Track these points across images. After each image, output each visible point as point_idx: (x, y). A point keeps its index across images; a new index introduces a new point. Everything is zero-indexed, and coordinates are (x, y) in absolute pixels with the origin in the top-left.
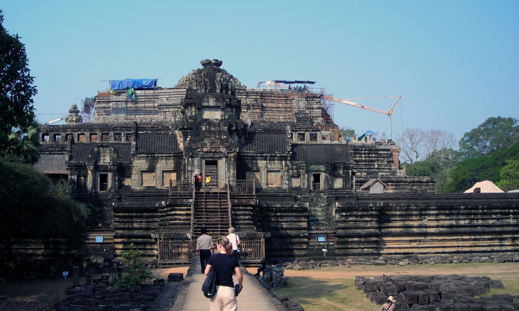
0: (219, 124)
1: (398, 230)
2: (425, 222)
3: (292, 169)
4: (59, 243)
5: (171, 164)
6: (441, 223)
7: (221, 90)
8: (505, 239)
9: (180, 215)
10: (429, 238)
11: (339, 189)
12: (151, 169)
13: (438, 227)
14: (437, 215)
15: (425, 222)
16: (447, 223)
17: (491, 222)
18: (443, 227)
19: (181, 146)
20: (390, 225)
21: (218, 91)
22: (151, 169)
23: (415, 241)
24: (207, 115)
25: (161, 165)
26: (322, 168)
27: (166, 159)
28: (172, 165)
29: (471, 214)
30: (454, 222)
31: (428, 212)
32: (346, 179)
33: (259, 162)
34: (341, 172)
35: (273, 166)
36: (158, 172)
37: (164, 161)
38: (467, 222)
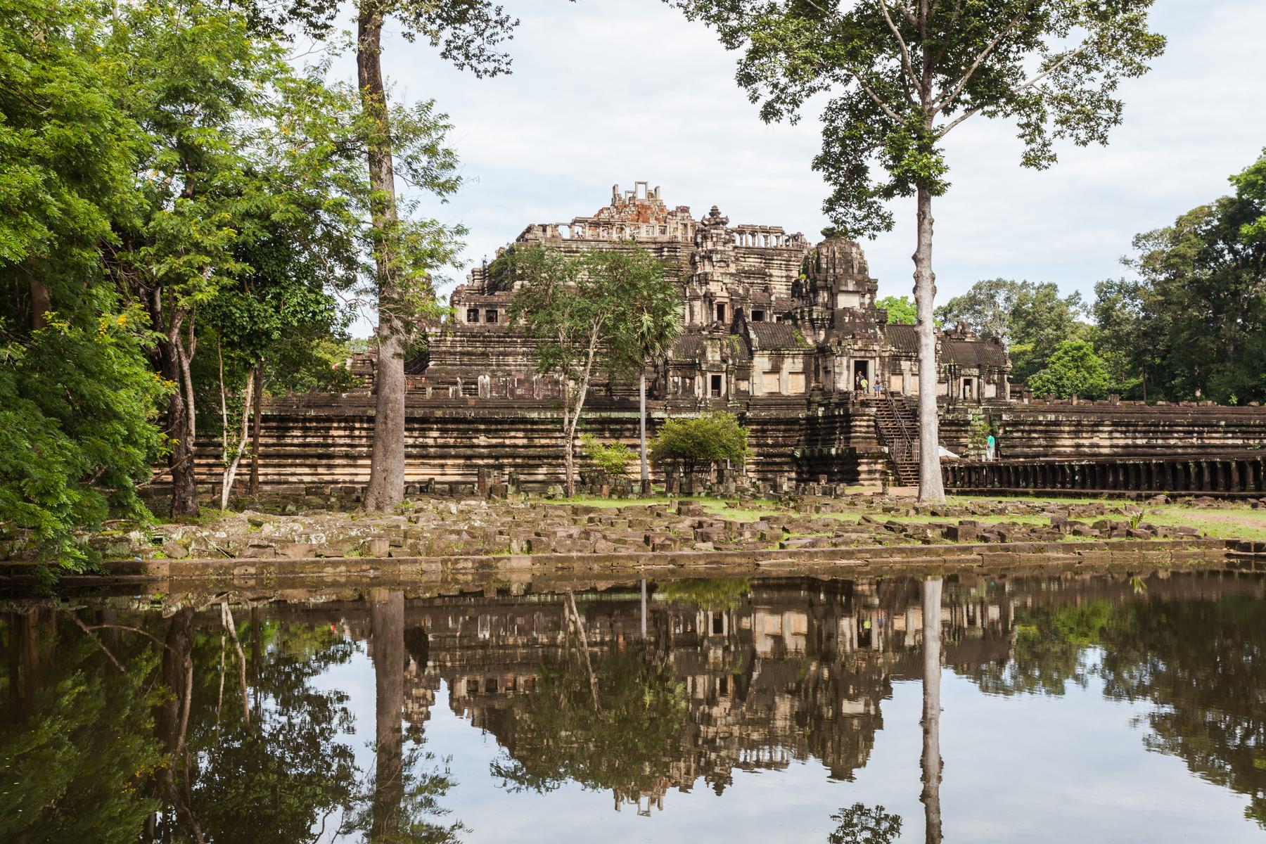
1: (1068, 450)
2: (1096, 440)
5: (799, 364)
6: (1115, 442)
12: (776, 370)
13: (1112, 446)
14: (1111, 432)
16: (1121, 442)
17: (1172, 442)
20: (1058, 443)
21: (856, 271)
22: (776, 370)
24: (843, 301)
25: (788, 365)
26: (976, 371)
28: (801, 366)
29: (1149, 432)
30: (1130, 442)
32: (1000, 386)
34: (996, 377)
36: (785, 373)
37: (790, 360)
38: (1144, 441)
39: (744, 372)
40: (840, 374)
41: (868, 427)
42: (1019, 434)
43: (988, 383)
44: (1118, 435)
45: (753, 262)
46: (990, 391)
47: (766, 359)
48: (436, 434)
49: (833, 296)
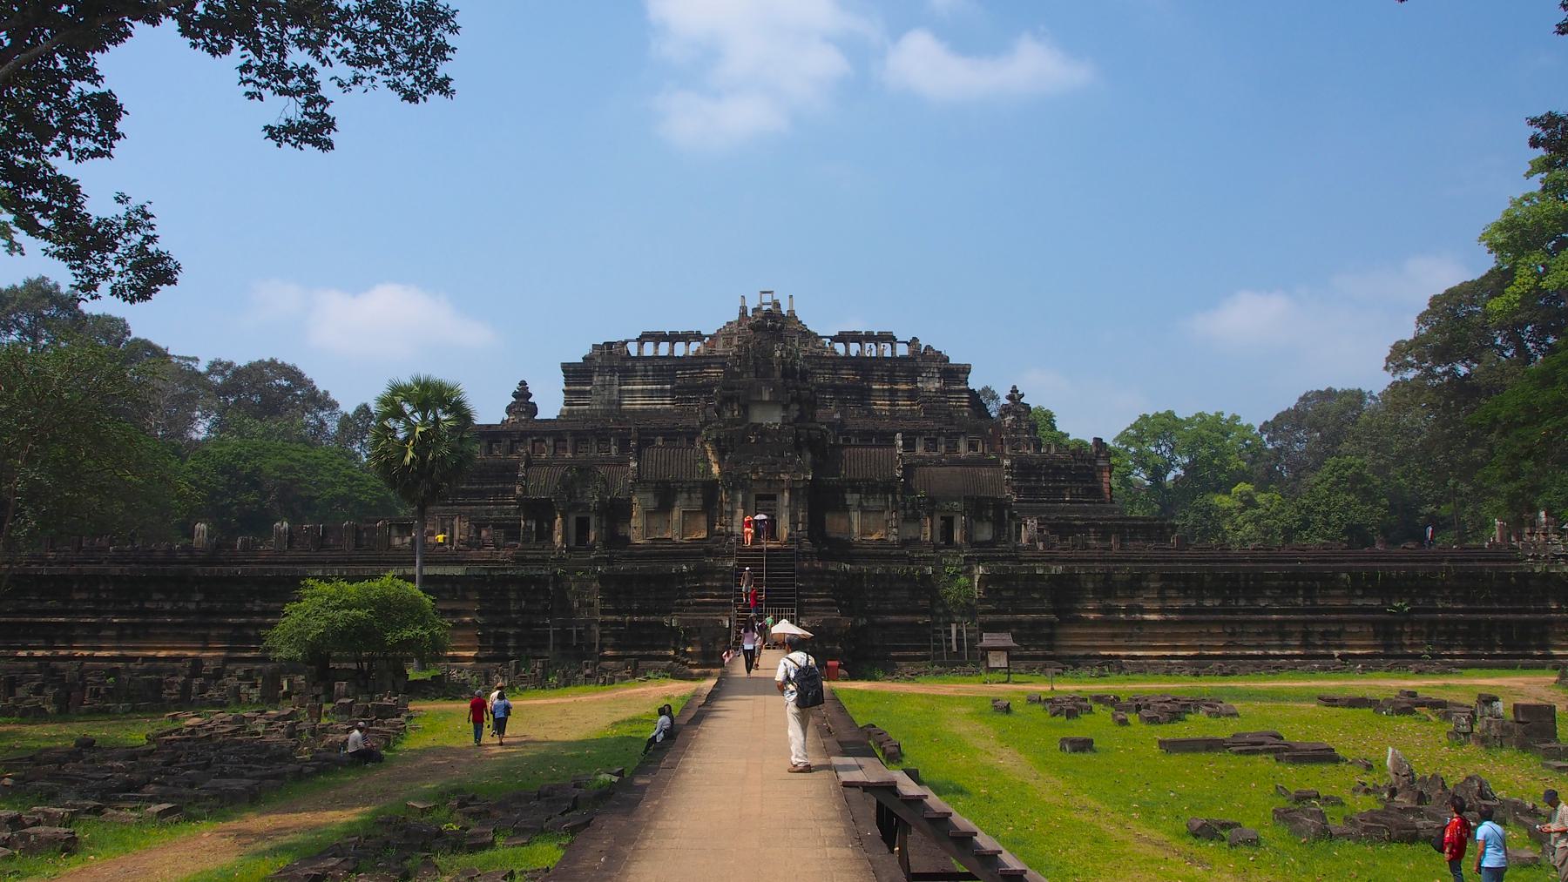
0: (779, 432)
2: (1139, 601)
3: (904, 508)
4: (506, 637)
5: (697, 503)
6: (1169, 603)
7: (784, 375)
8: (1290, 634)
9: (712, 588)
10: (1146, 630)
11: (986, 542)
12: (664, 507)
15: (1139, 601)
16: (1179, 604)
18: (1173, 611)
19: (715, 469)
21: (777, 374)
23: (1122, 635)
27: (689, 492)
28: (700, 502)
31: (1144, 584)
33: (848, 496)
35: (871, 503)
39: (617, 512)
40: (733, 513)
41: (723, 588)
42: (1011, 593)
43: (980, 519)
44: (1173, 593)
45: (847, 375)
46: (985, 533)
47: (650, 495)
48: (198, 597)
49: (745, 408)
